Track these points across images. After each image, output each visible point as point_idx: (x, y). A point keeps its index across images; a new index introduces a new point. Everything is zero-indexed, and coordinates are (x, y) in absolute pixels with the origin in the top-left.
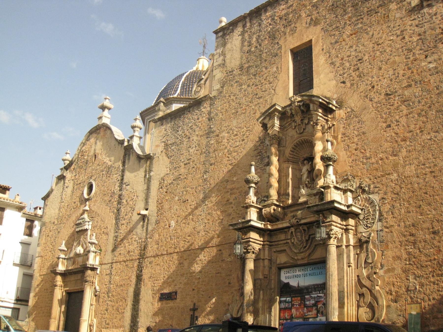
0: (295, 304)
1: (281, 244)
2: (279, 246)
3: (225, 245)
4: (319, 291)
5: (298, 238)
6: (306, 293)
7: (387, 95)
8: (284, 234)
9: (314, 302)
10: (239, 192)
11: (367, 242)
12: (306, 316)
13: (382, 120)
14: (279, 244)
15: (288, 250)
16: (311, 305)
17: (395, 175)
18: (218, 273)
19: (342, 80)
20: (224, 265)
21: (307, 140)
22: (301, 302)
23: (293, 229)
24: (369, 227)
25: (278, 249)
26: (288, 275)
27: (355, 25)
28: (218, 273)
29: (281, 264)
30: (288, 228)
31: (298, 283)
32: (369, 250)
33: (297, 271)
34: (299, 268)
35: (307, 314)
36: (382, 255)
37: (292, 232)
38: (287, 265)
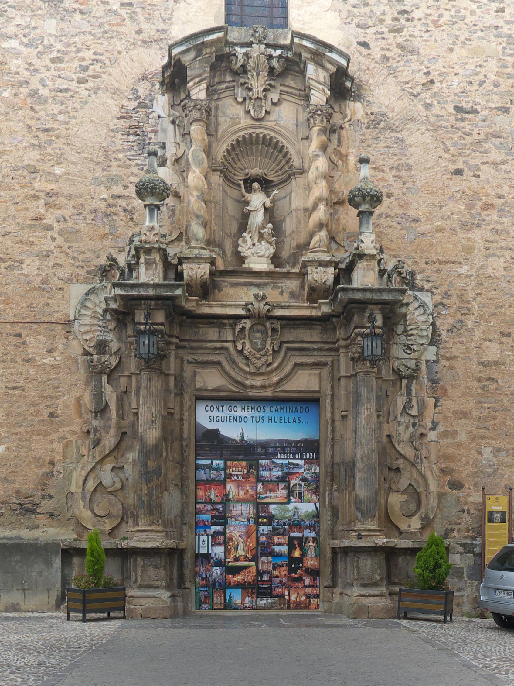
0: (234, 473)
3: (35, 326)
4: (294, 454)
5: (256, 343)
6: (260, 454)
7: (458, 109)
8: (217, 330)
9: (280, 473)
10: (74, 207)
11: (411, 378)
12: (263, 498)
13: (447, 156)
15: (225, 364)
16: (274, 479)
17: (466, 267)
18: (15, 388)
19: (362, 39)
20: (32, 372)
21: (271, 138)
22: (249, 471)
24: (415, 351)
25: (200, 358)
26: (215, 414)
28: (15, 388)
29: (206, 390)
31: (242, 434)
32: (413, 393)
33: (239, 409)
34: (245, 404)
35: (264, 496)
36: (436, 406)
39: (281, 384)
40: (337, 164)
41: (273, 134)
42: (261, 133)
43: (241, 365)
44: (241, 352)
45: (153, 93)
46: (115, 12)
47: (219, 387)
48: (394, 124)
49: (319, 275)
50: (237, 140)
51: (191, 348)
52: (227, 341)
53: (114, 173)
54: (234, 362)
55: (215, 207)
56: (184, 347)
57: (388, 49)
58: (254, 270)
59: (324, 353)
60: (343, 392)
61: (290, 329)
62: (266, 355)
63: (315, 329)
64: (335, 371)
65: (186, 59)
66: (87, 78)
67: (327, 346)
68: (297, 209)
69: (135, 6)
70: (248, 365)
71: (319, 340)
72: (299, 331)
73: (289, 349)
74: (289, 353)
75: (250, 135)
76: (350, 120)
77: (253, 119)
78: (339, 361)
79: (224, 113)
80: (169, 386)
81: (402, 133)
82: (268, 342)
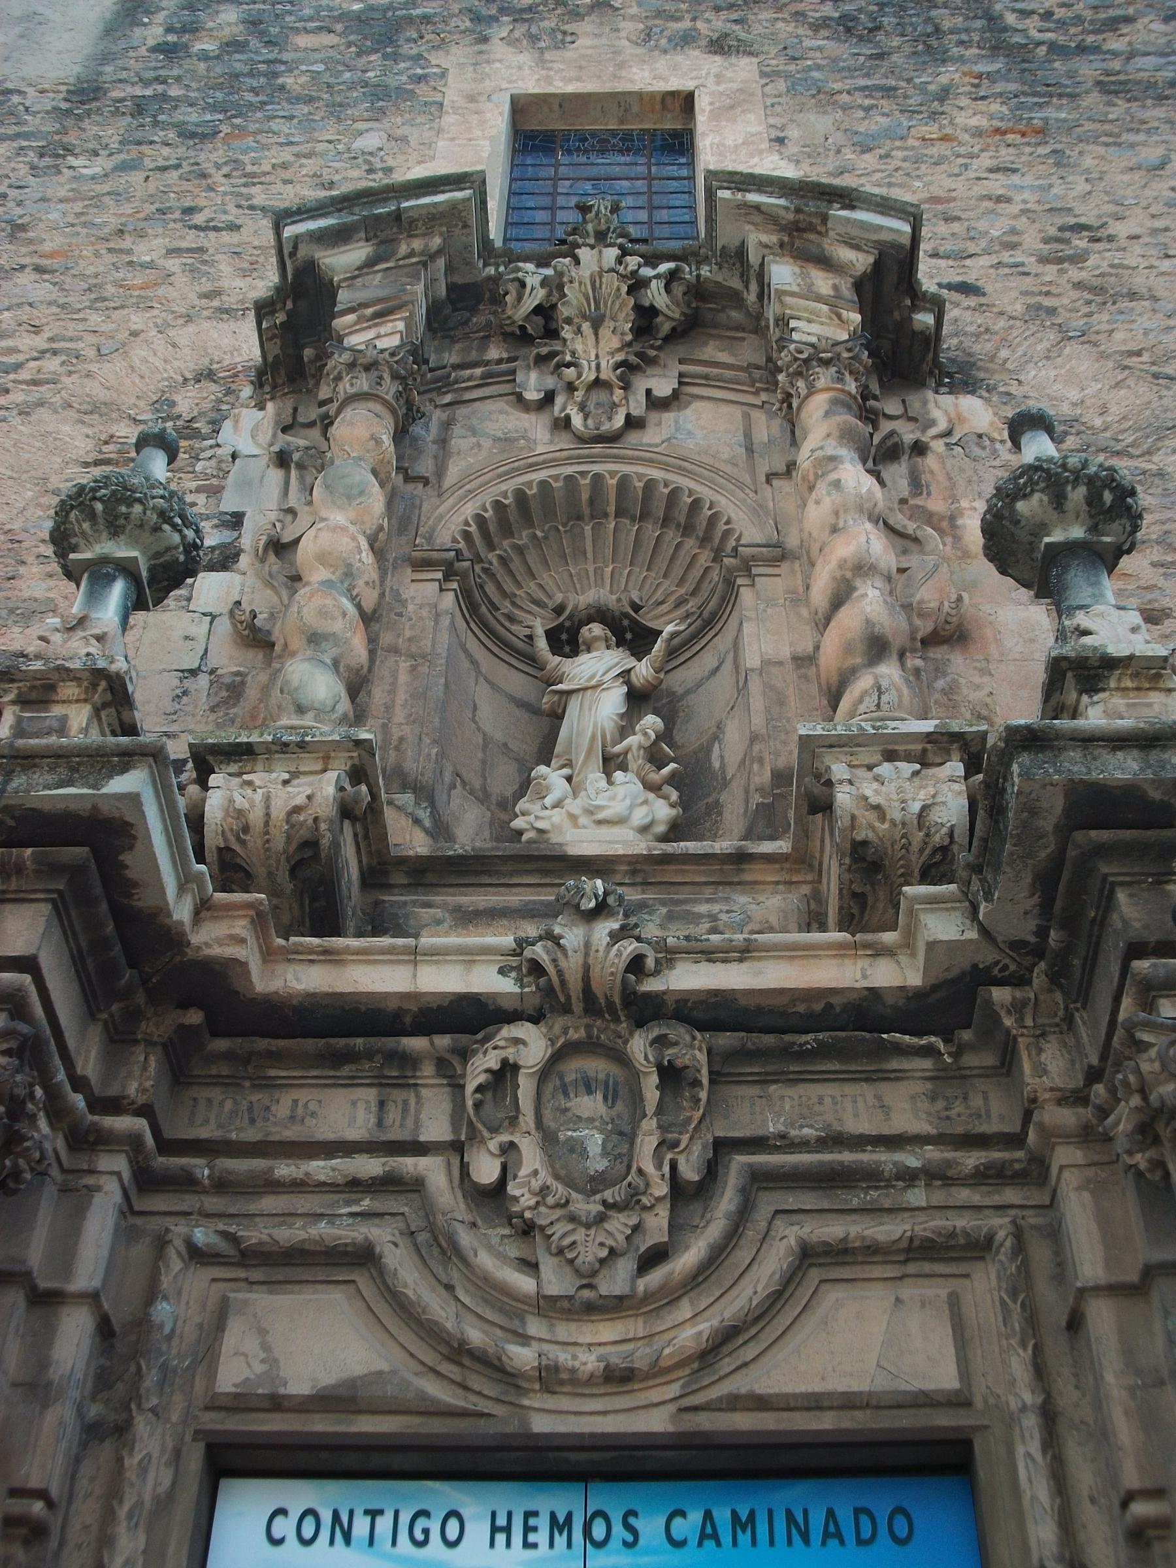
1: (299, 1186)
2: (269, 1203)
5: (577, 1148)
8: (370, 1095)
14: (274, 1186)
15: (399, 1260)
21: (650, 485)
23: (531, 1045)
25: (255, 1235)
27: (1020, 106)
29: (277, 1403)
30: (471, 1017)
33: (478, 1530)
34: (510, 1499)
37: (506, 1072)
38: (367, 1425)
39: (727, 1365)
40: (919, 534)
41: (656, 473)
42: (612, 474)
43: (485, 1260)
44: (492, 1198)
45: (224, 407)
46: (150, 265)
47: (352, 1383)
48: (1118, 441)
49: (890, 789)
50: (520, 495)
51: (221, 1185)
52: (419, 1149)
53: (26, 594)
54: (451, 1251)
55: (413, 668)
56: (186, 1182)
57: (1047, 294)
58: (573, 851)
59: (964, 1195)
60: (1114, 1380)
61: (764, 1080)
62: (632, 1201)
63: (898, 1076)
64: (1045, 1292)
65: (341, 260)
66: (10, 385)
67: (971, 1160)
68: (766, 663)
69: (211, 251)
70: (530, 1266)
71: (923, 1126)
72: (814, 1090)
73: (760, 1180)
74: (768, 1202)
75: (569, 478)
76: (948, 433)
77: (581, 439)
78: (1055, 1234)
79: (473, 431)
80: (44, 1364)
81: (1156, 459)
82: (647, 1143)
